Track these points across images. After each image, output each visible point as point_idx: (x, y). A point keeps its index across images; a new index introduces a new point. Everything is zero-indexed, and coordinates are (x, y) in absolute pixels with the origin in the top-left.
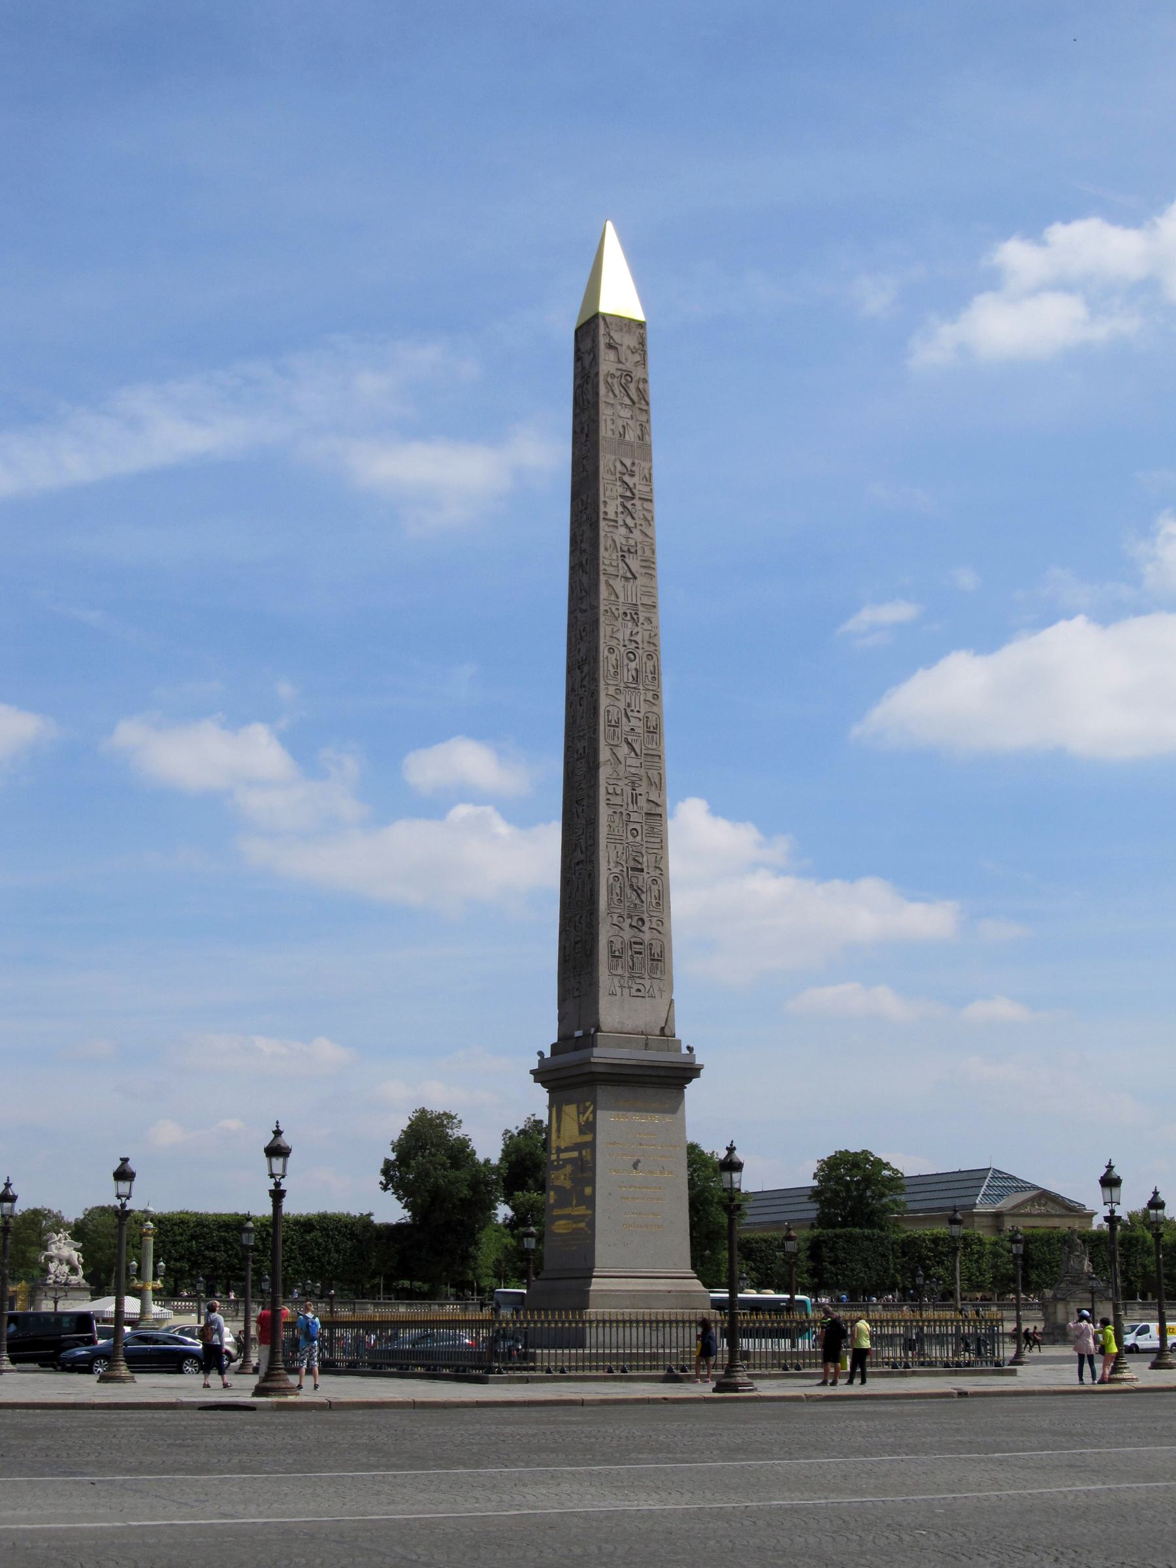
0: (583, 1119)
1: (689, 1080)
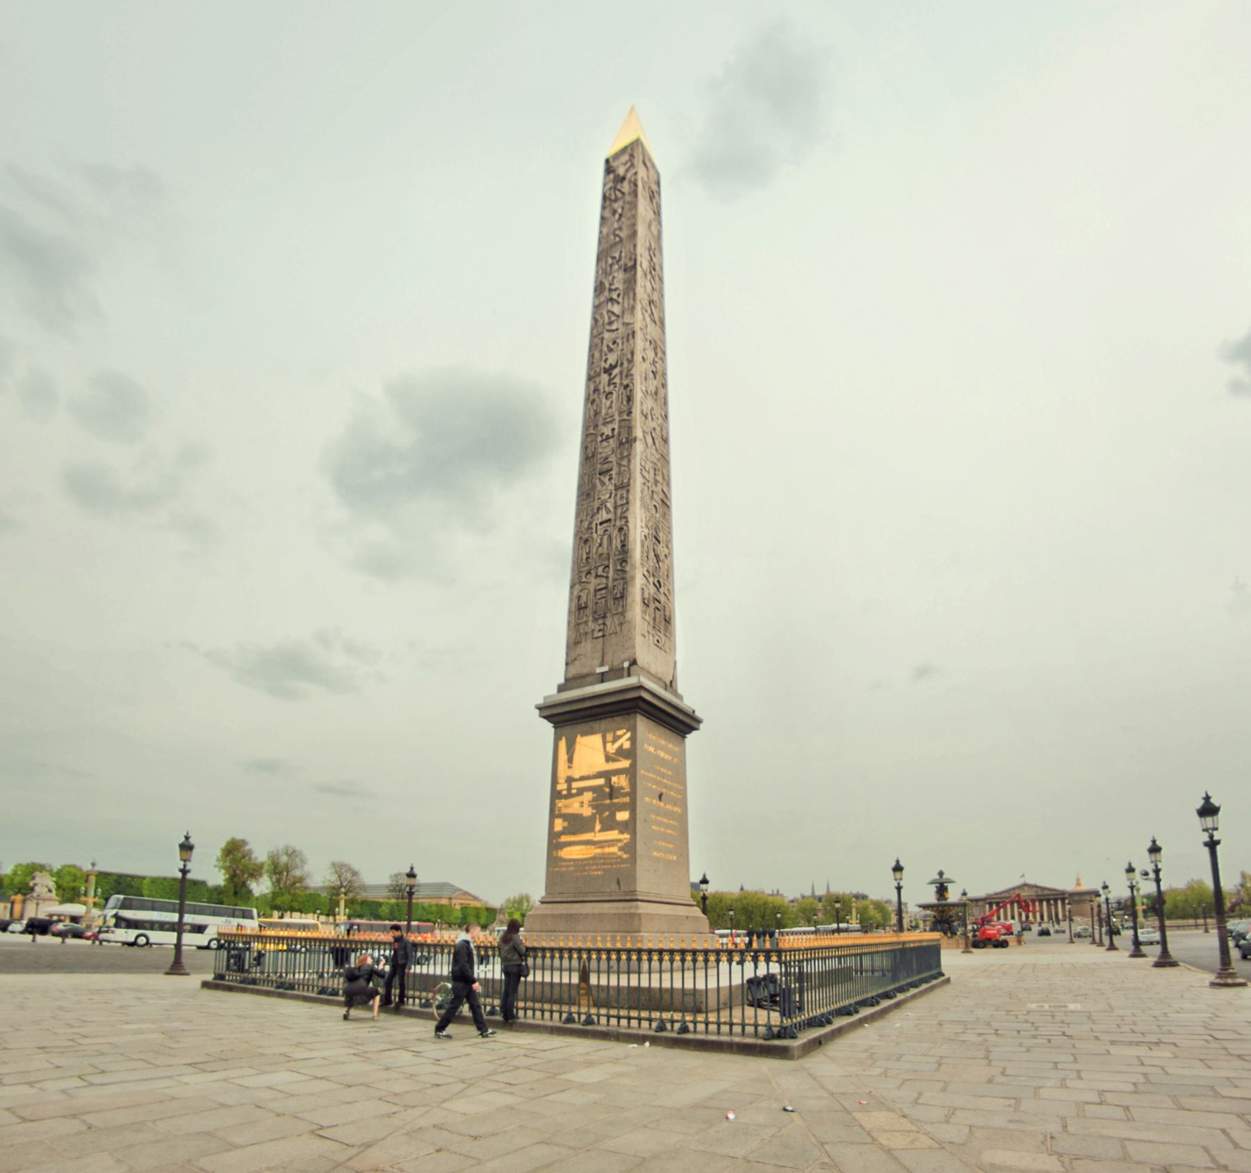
0: (611, 748)
1: (689, 733)
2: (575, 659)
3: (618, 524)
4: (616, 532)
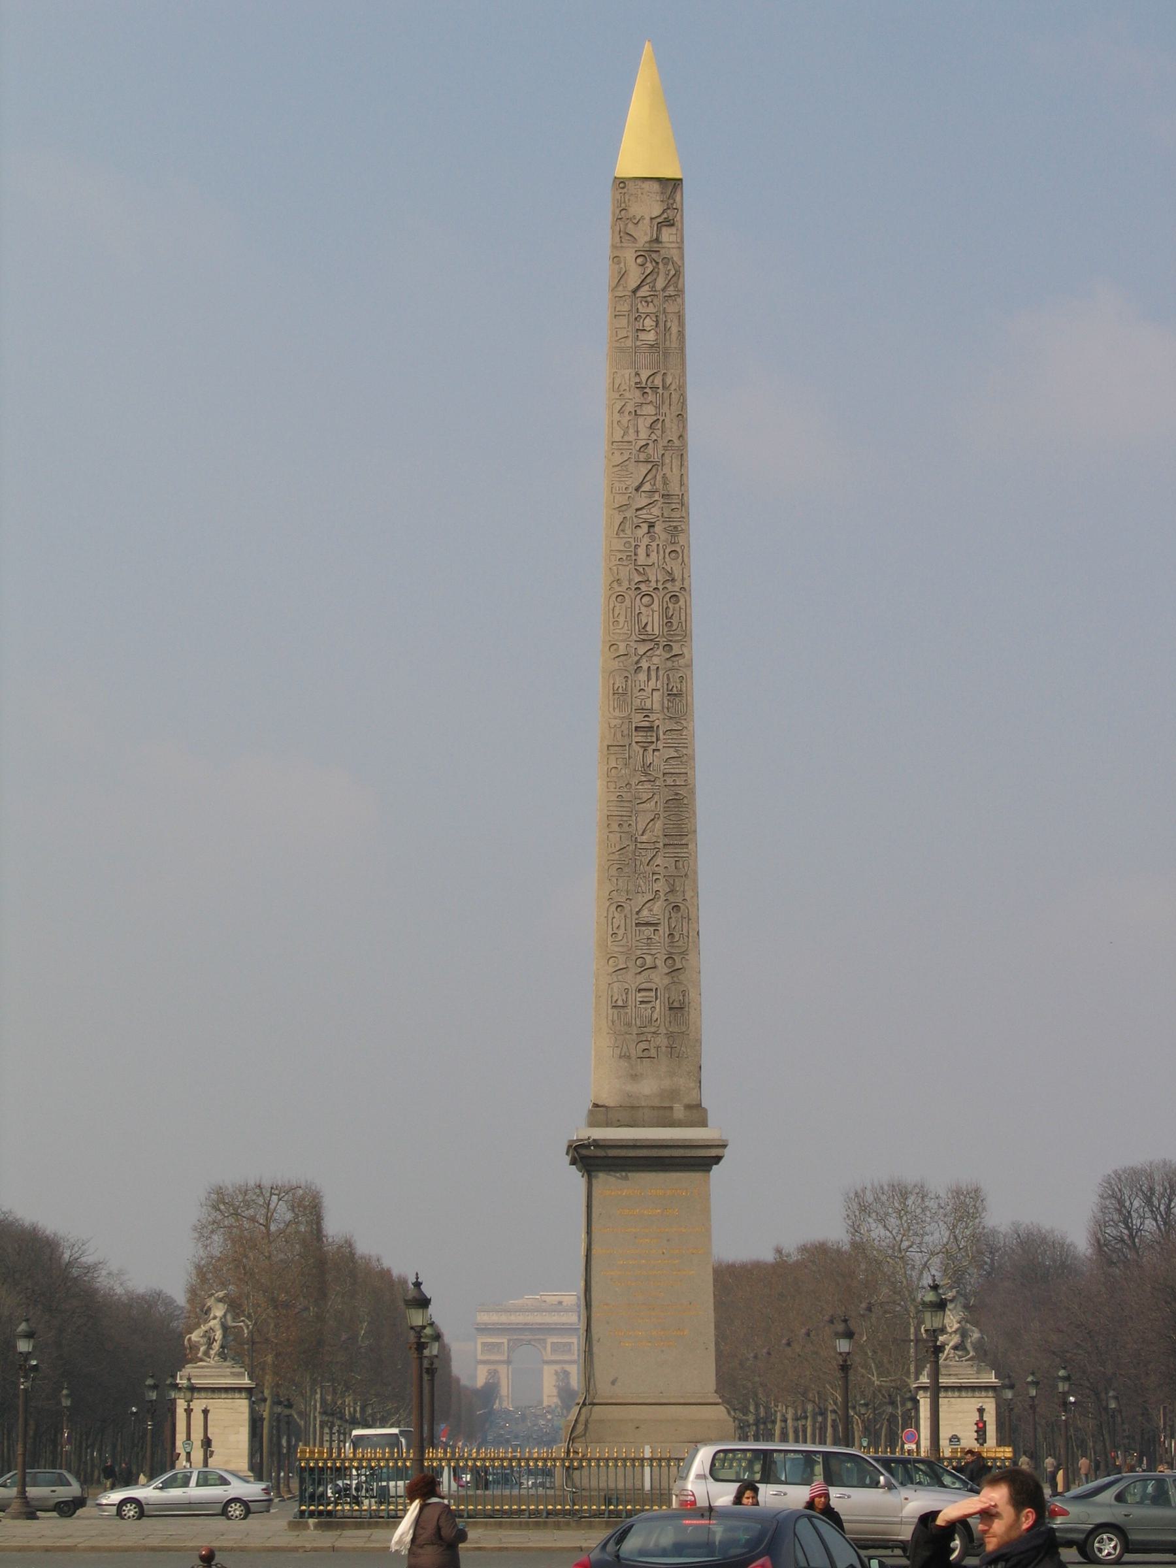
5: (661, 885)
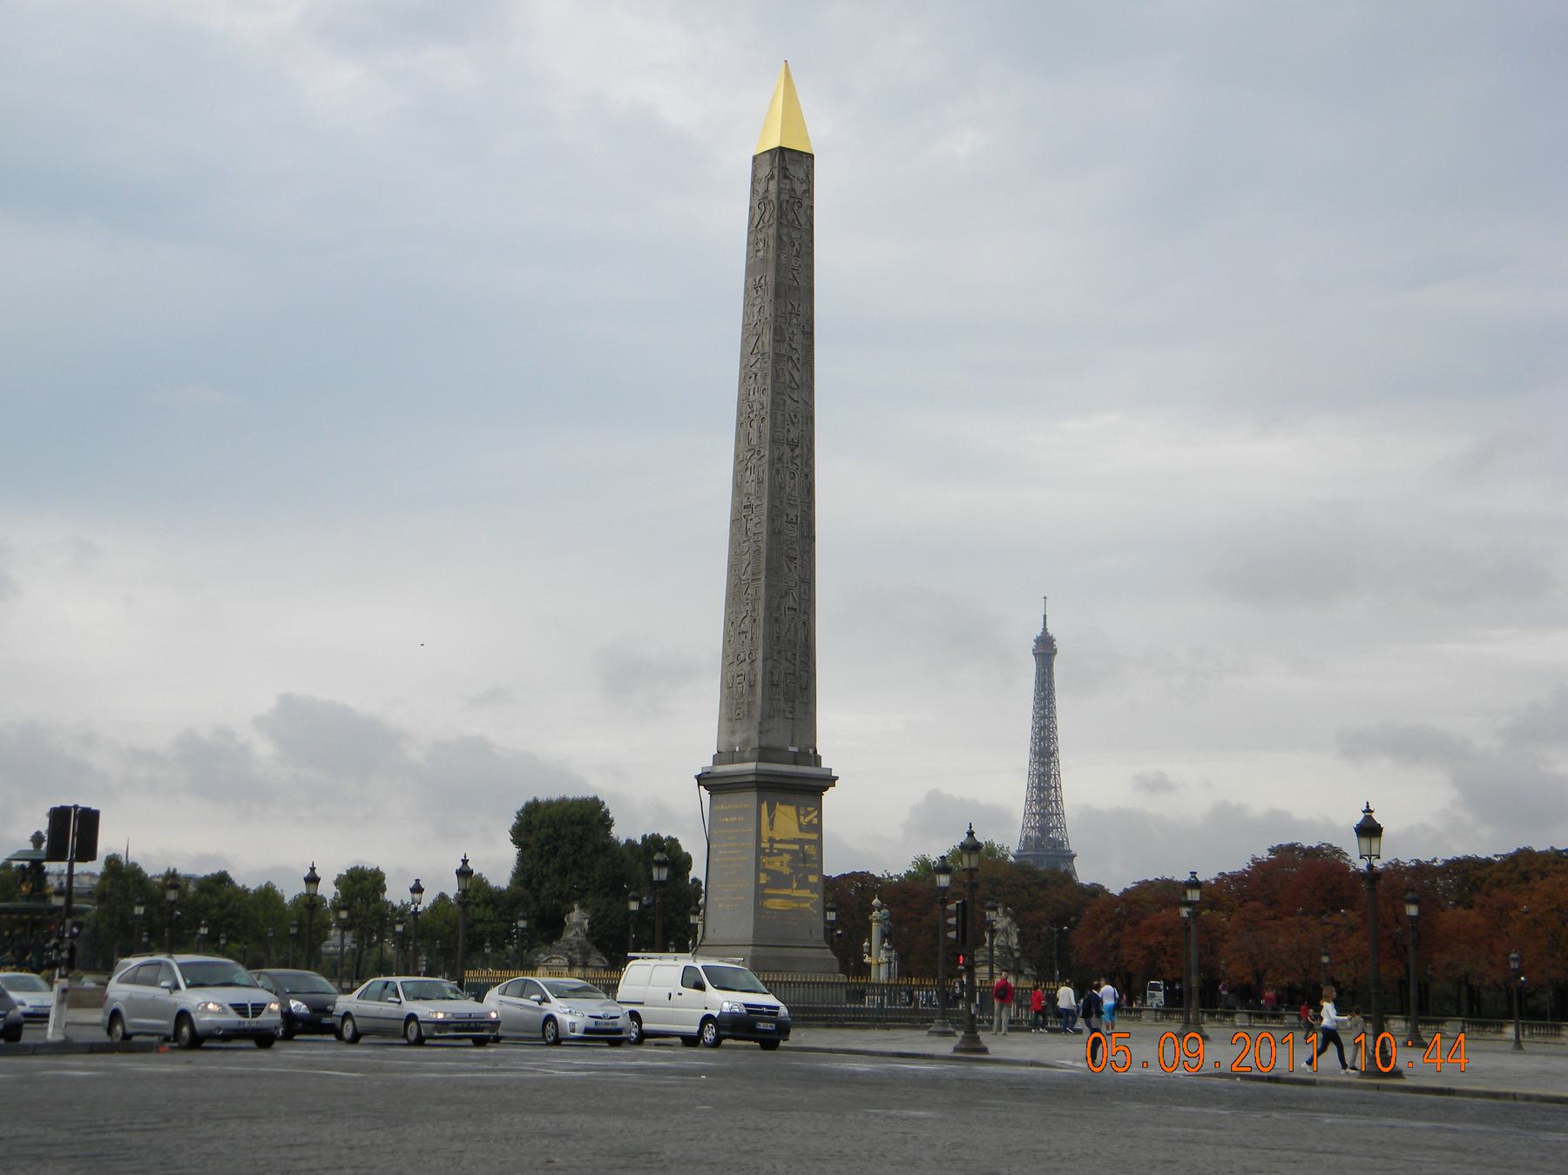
0: (804, 821)
2: (768, 731)
3: (804, 617)
4: (800, 625)
5: (749, 608)
